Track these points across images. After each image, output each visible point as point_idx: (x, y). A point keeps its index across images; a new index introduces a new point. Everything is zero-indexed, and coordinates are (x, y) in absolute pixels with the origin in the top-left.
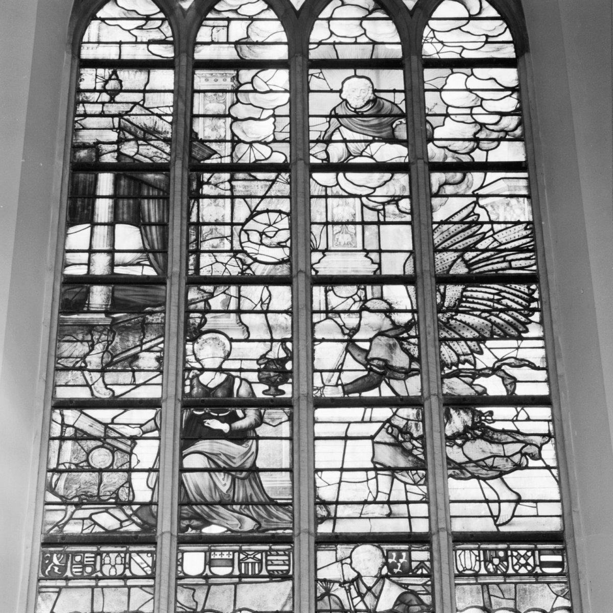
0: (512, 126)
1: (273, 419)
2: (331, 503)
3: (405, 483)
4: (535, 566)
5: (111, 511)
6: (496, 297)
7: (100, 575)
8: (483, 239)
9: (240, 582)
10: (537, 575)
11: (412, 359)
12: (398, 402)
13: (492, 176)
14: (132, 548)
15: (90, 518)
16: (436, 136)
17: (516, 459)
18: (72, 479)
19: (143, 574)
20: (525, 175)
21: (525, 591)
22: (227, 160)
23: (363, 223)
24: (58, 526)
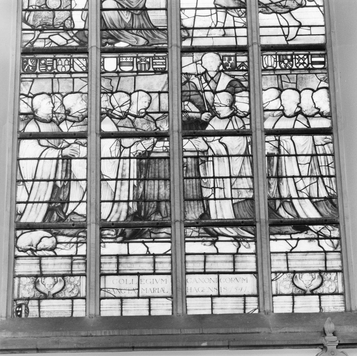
2: (190, 29)
3: (234, 16)
4: (309, 64)
5: (61, 34)
7: (56, 71)
9: (138, 75)
10: (309, 69)
14: (74, 56)
15: (49, 38)
18: (37, 15)
19: (81, 70)
21: (302, 78)
24: (30, 43)
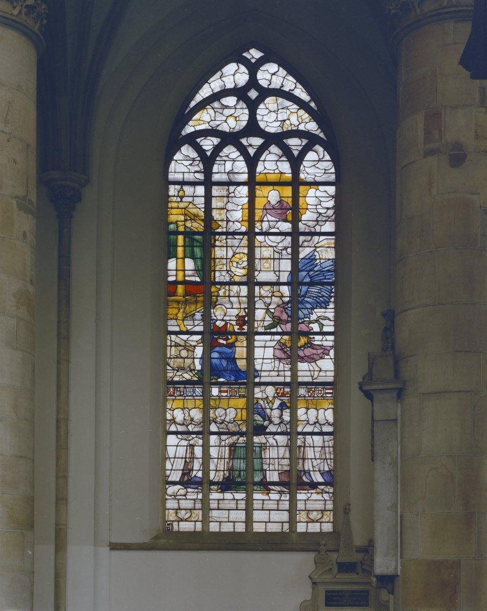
0: (331, 215)
1: (241, 340)
2: (259, 371)
6: (319, 291)
8: (317, 266)
11: (288, 316)
12: (282, 334)
13: (322, 238)
16: (302, 219)
17: (321, 355)
20: (334, 237)
22: (224, 230)
23: (274, 259)
